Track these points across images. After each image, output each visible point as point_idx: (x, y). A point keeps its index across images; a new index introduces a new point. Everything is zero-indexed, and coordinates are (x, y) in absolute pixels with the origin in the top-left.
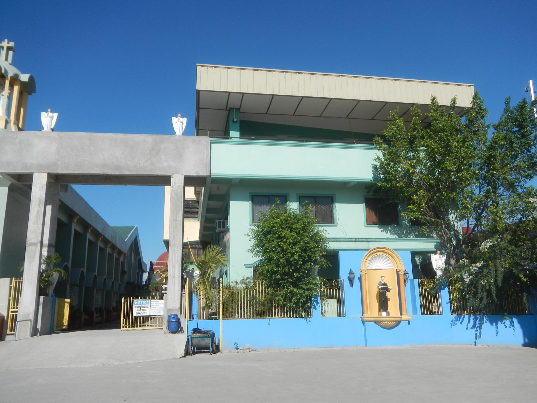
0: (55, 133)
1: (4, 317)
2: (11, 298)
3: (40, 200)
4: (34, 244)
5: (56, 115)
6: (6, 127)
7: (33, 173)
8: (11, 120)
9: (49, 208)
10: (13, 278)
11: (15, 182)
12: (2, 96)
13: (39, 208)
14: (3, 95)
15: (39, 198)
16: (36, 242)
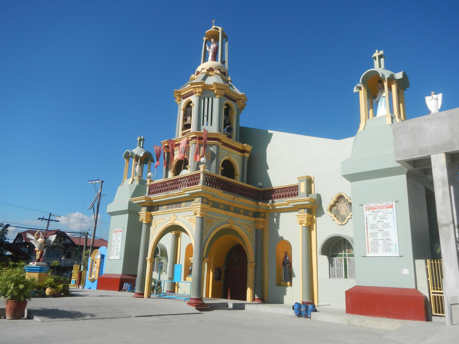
0: (444, 113)
1: (426, 297)
2: (429, 279)
3: (443, 181)
4: (447, 225)
5: (440, 96)
6: (392, 122)
7: (430, 155)
8: (395, 115)
9: (452, 187)
10: (428, 260)
11: (411, 168)
12: (383, 98)
13: (444, 189)
14: (384, 97)
15: (441, 179)
16: (448, 223)
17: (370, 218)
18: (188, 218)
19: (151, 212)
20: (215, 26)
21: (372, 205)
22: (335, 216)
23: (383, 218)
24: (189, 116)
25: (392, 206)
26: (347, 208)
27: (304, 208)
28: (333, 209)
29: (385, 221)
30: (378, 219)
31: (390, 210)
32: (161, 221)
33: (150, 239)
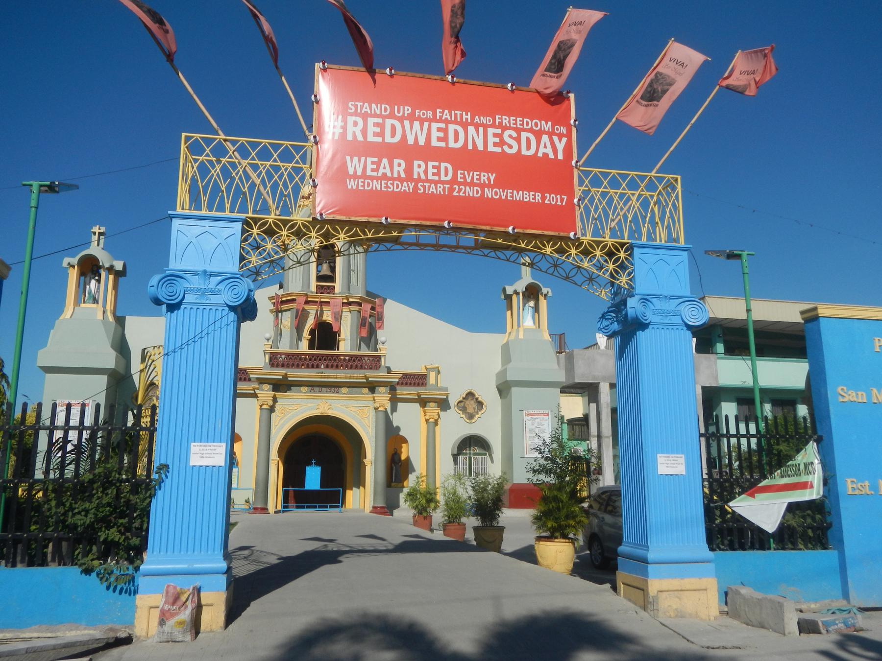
3: (607, 404)
4: (608, 437)
7: (599, 383)
17: (529, 423)
18: (353, 409)
19: (276, 393)
21: (531, 412)
22: (463, 414)
23: (540, 424)
24: (326, 262)
25: (548, 415)
26: (475, 406)
27: (435, 402)
28: (459, 405)
29: (542, 427)
30: (536, 425)
31: (546, 418)
32: (296, 408)
33: (273, 431)
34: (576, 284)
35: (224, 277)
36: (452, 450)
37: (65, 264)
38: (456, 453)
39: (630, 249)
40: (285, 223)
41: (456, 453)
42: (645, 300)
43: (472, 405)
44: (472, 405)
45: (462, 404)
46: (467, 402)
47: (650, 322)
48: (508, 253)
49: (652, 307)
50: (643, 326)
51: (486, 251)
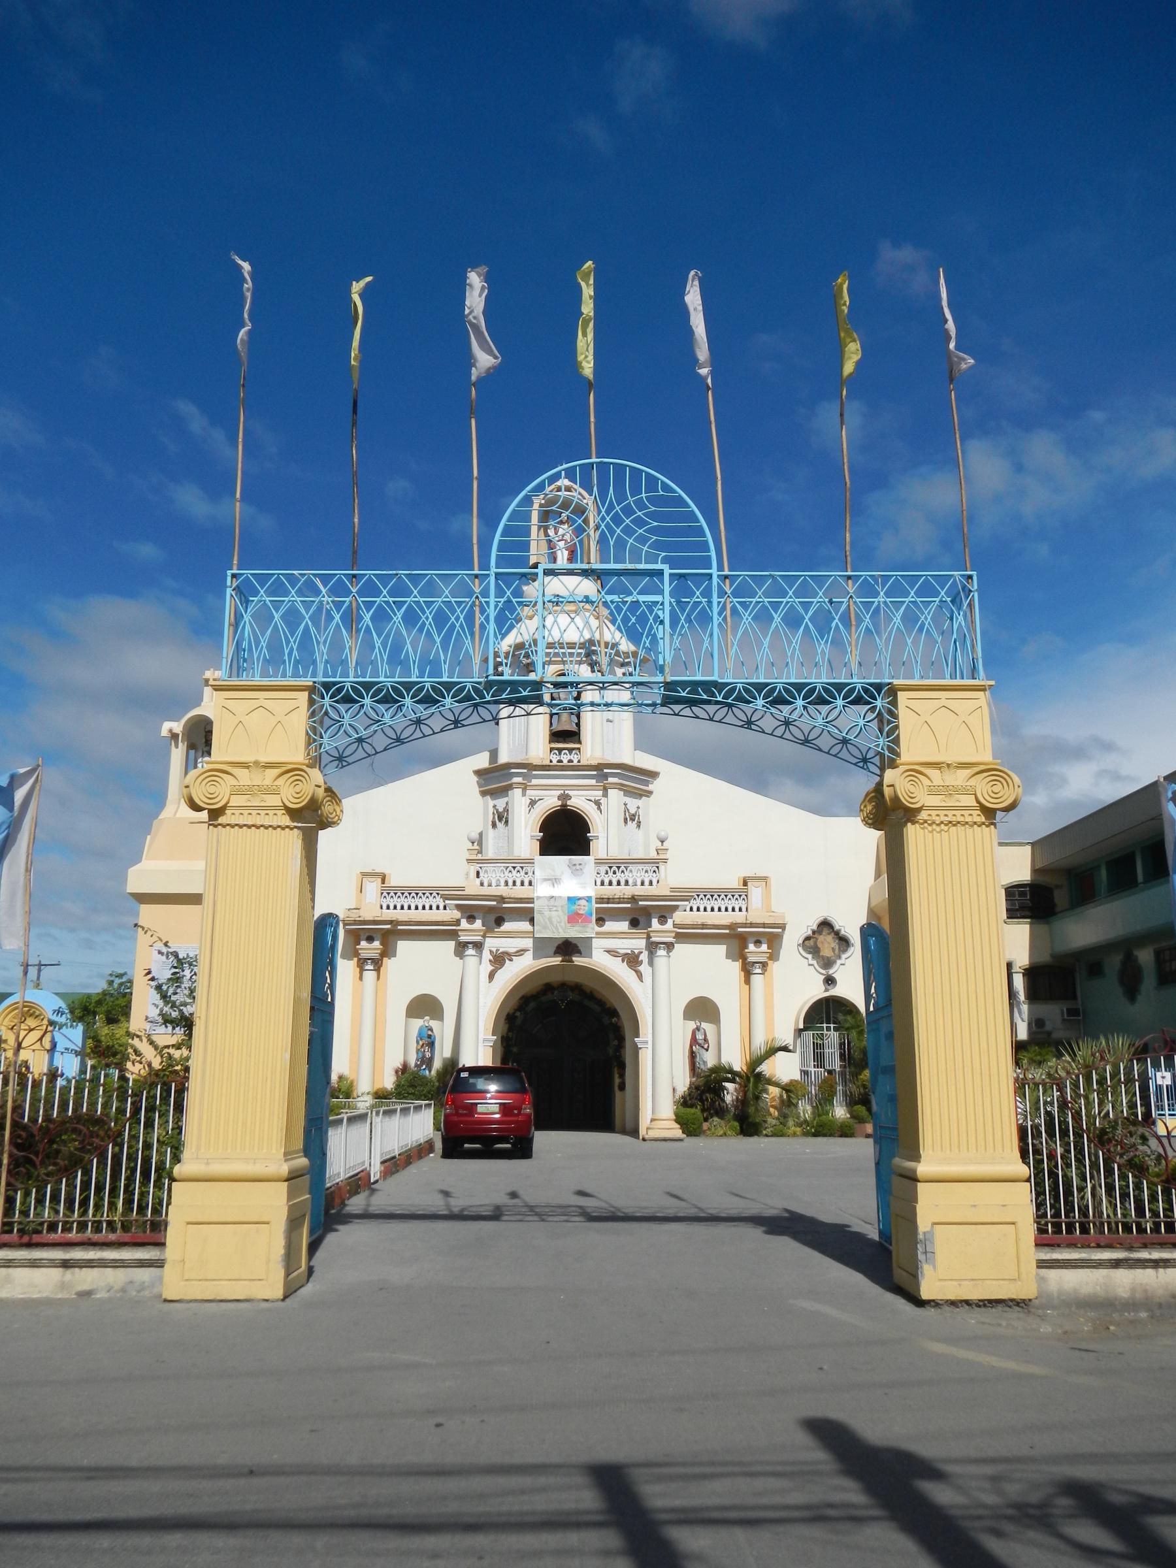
20: (572, 484)
22: (813, 958)
28: (806, 942)
34: (820, 750)
35: (284, 769)
36: (797, 1022)
37: (164, 732)
38: (801, 1026)
39: (893, 692)
40: (368, 686)
41: (801, 1026)
42: (915, 771)
43: (829, 943)
44: (829, 943)
45: (812, 942)
46: (821, 938)
47: (923, 806)
48: (711, 709)
49: (926, 782)
50: (910, 814)
51: (677, 708)
